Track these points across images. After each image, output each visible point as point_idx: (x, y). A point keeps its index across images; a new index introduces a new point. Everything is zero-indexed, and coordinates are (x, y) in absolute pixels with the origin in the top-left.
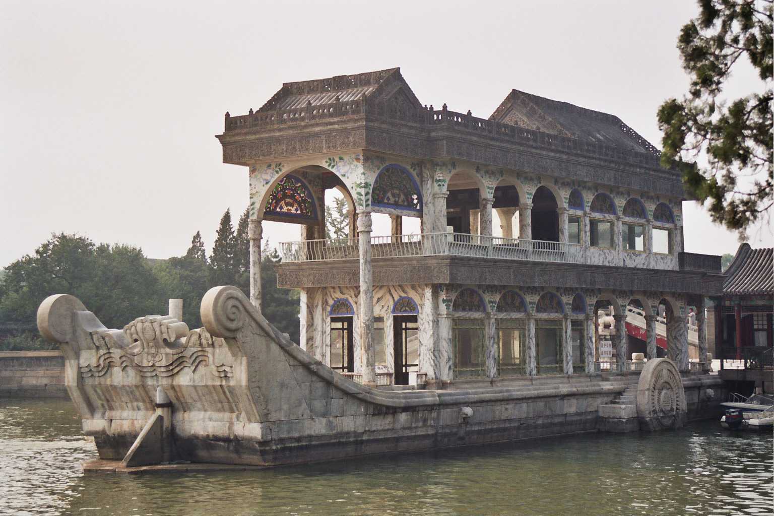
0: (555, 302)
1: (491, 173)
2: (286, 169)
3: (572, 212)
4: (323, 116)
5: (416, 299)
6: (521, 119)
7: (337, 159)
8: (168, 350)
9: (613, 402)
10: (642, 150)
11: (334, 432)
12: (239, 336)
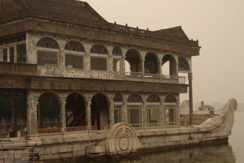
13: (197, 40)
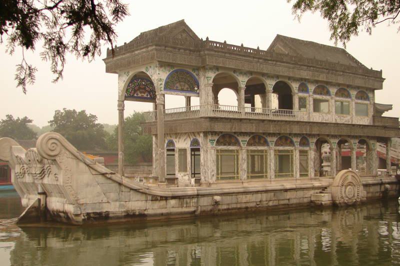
0: (288, 142)
2: (132, 73)
3: (301, 94)
4: (140, 46)
6: (281, 48)
7: (149, 68)
9: (321, 193)
10: (347, 62)
11: (125, 210)
12: (57, 159)
13: (381, 71)
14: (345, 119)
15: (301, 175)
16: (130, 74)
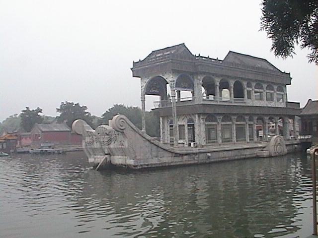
1: (217, 76)
3: (248, 89)
5: (194, 119)
8: (107, 136)
12: (124, 131)
14: (272, 104)
15: (250, 140)
16: (150, 78)
